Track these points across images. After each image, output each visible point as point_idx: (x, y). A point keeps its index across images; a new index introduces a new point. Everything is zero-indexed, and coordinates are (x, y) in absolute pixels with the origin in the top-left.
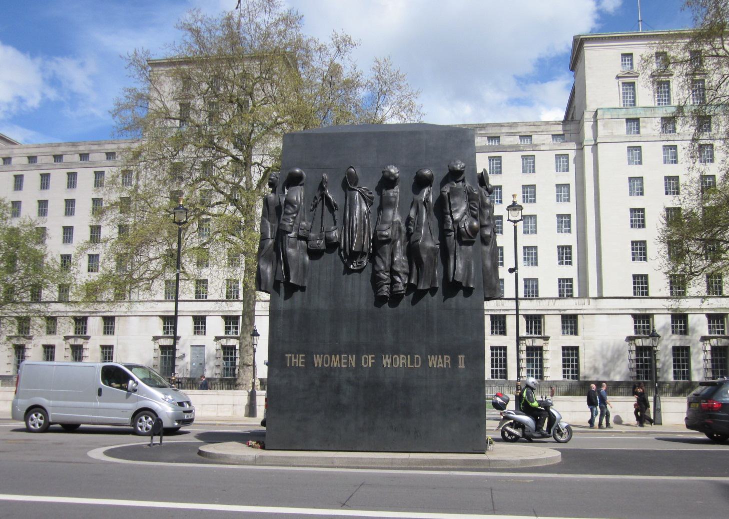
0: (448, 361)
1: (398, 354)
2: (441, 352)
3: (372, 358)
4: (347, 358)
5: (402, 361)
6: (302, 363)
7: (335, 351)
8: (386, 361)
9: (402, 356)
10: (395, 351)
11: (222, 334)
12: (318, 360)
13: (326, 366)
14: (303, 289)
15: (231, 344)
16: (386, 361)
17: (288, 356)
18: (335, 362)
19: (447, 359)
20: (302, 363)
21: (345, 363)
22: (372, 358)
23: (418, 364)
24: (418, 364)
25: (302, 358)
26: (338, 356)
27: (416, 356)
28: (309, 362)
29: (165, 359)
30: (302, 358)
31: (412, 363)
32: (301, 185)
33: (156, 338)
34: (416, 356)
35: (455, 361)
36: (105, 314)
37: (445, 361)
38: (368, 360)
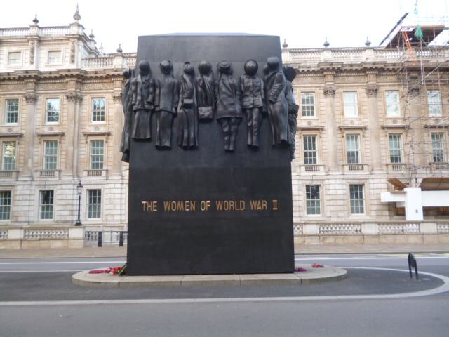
0: (265, 205)
1: (228, 200)
3: (208, 204)
5: (232, 204)
6: (155, 208)
8: (219, 205)
9: (231, 202)
12: (167, 206)
13: (174, 210)
16: (219, 205)
17: (144, 202)
18: (180, 206)
19: (264, 203)
20: (155, 208)
21: (187, 208)
22: (208, 204)
23: (242, 207)
24: (242, 207)
25: (155, 204)
26: (182, 203)
27: (241, 202)
28: (160, 206)
30: (155, 204)
31: (238, 207)
34: (241, 202)
35: (270, 205)
37: (263, 205)
38: (207, 204)
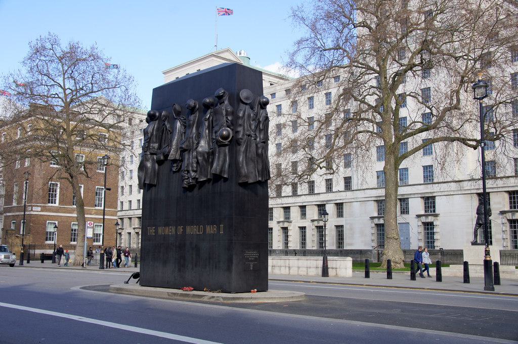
0: (215, 229)
2: (213, 223)
4: (171, 229)
7: (167, 225)
8: (189, 230)
10: (192, 224)
11: (423, 212)
14: (155, 186)
15: (429, 221)
17: (149, 228)
28: (156, 232)
29: (428, 234)
32: (156, 120)
33: (372, 218)
36: (336, 202)
37: (214, 229)
